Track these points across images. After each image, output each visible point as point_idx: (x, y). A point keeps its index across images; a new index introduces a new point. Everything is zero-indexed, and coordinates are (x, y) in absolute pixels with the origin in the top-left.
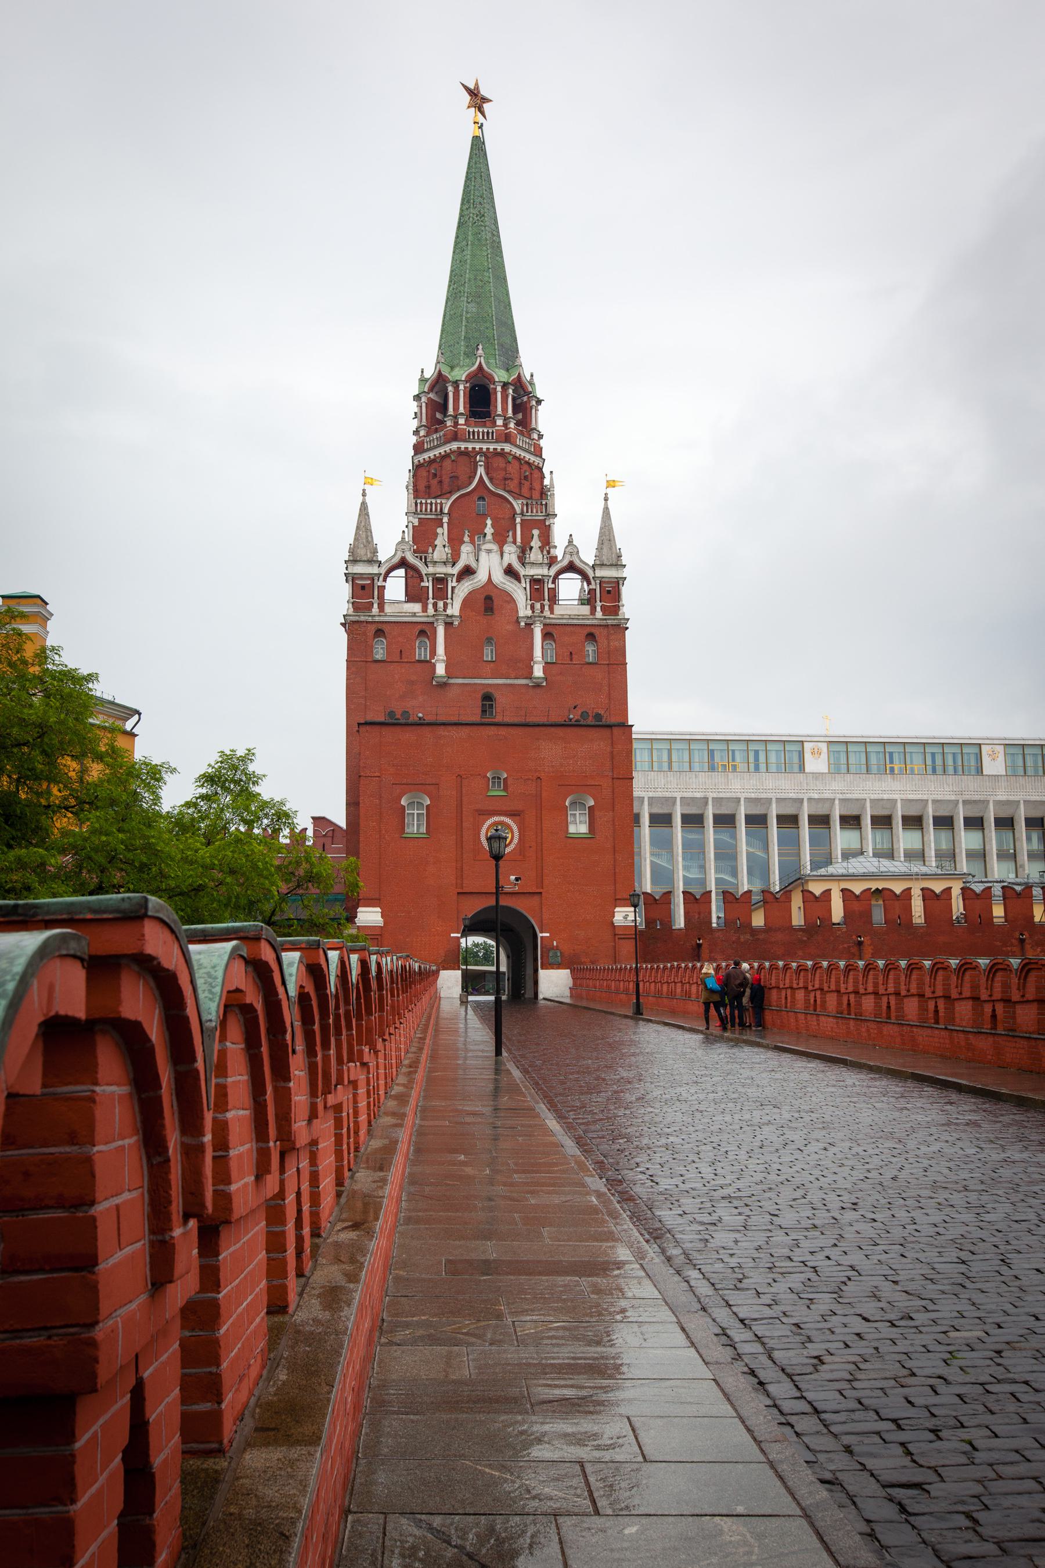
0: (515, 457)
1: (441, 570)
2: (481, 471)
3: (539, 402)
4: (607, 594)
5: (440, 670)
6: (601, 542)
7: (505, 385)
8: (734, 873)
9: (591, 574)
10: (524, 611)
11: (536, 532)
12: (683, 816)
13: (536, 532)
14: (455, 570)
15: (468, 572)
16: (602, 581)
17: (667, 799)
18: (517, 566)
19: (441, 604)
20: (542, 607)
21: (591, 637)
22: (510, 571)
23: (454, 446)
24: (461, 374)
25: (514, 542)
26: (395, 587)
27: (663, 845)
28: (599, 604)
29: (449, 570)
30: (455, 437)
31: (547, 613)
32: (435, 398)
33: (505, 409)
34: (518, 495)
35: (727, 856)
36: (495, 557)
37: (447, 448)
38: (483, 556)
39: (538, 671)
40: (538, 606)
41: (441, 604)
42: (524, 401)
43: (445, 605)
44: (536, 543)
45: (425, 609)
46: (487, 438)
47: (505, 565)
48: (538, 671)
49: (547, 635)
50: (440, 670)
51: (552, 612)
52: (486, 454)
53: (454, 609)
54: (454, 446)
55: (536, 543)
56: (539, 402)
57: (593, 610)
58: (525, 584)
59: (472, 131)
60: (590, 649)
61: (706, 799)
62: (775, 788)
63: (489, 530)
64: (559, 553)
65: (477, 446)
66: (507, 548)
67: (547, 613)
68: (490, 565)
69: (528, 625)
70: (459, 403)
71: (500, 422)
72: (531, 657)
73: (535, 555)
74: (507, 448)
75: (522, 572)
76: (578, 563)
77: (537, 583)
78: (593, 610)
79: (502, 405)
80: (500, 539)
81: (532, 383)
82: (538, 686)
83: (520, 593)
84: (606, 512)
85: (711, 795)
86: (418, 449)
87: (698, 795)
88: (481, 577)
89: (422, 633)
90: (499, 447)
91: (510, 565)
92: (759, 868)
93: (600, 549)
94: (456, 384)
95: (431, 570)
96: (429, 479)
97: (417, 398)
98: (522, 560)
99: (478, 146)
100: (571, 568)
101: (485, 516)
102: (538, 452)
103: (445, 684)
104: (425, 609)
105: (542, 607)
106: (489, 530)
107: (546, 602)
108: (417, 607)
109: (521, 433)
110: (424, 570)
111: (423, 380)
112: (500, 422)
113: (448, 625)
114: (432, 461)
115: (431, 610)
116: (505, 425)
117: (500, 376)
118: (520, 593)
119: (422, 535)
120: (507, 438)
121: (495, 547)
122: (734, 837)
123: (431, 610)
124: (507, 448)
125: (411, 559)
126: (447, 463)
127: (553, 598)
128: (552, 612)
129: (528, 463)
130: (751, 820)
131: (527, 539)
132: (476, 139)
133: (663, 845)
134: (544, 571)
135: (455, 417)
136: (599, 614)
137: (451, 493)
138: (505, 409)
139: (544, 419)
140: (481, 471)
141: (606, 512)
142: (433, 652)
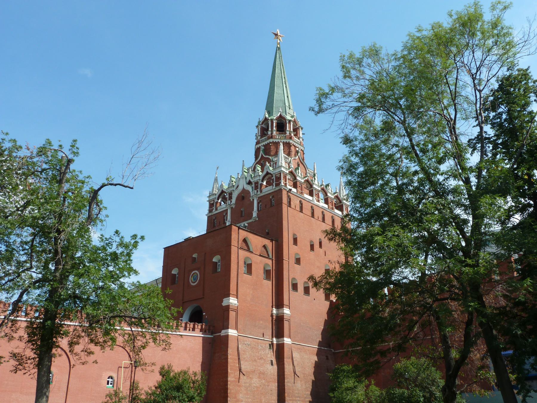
2: (261, 152)
19: (229, 201)
20: (257, 191)
28: (274, 184)
29: (233, 189)
31: (259, 193)
40: (256, 191)
43: (231, 202)
46: (266, 140)
47: (248, 181)
58: (253, 185)
65: (262, 144)
67: (259, 193)
69: (253, 200)
76: (269, 172)
77: (256, 183)
88: (240, 188)
90: (268, 141)
91: (250, 180)
105: (257, 191)
107: (259, 190)
112: (269, 133)
124: (271, 140)
136: (274, 187)
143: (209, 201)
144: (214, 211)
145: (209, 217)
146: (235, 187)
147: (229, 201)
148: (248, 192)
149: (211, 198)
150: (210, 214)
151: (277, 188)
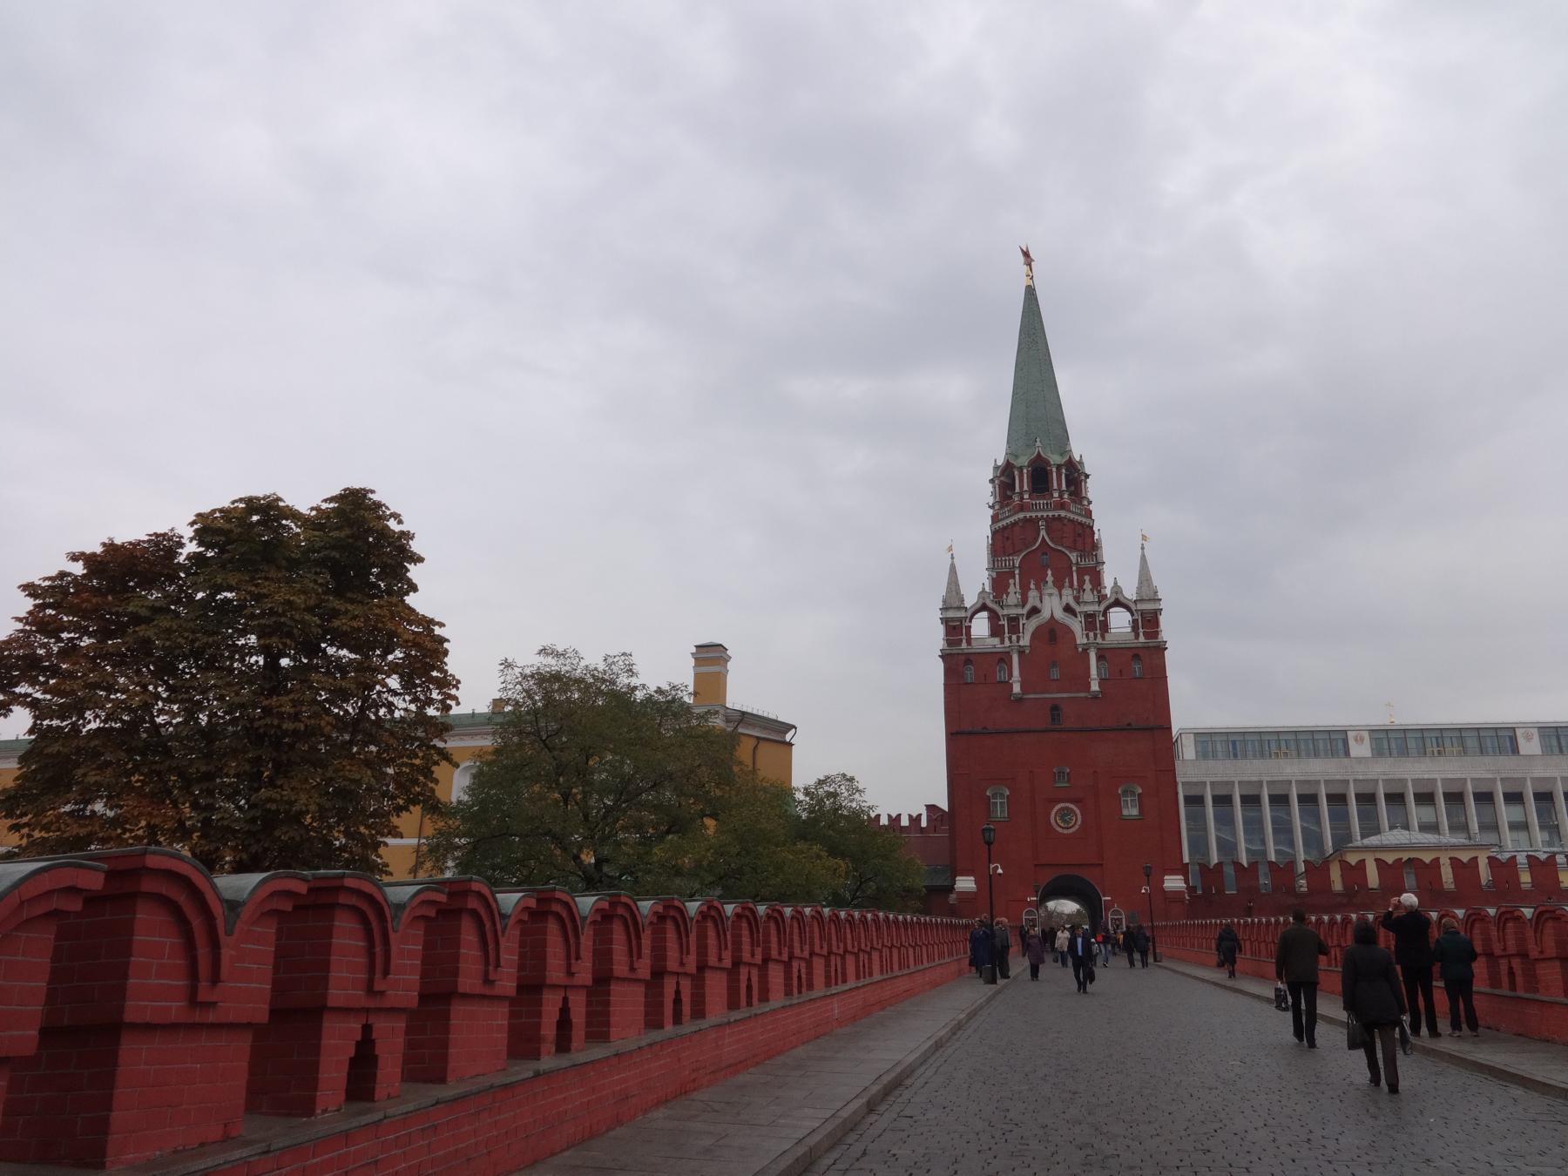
0: (1070, 520)
1: (1013, 612)
2: (1043, 533)
3: (1087, 476)
4: (1148, 621)
5: (1017, 688)
6: (1141, 582)
7: (1059, 467)
8: (1292, 844)
9: (1133, 607)
10: (1081, 639)
11: (1087, 578)
12: (1242, 797)
13: (1087, 578)
14: (1025, 611)
15: (1035, 611)
16: (1143, 613)
17: (1227, 783)
18: (1073, 604)
21: (1136, 657)
22: (1068, 609)
23: (1021, 515)
24: (1023, 461)
25: (1071, 586)
26: (980, 627)
27: (1225, 820)
30: (1022, 508)
32: (1005, 479)
33: (1060, 484)
34: (1073, 548)
35: (1283, 829)
36: (1056, 599)
37: (1016, 517)
38: (1046, 598)
39: (1095, 687)
41: (1014, 637)
42: (1075, 475)
44: (1088, 586)
45: (1002, 642)
46: (1047, 507)
48: (1095, 687)
49: (1100, 658)
50: (1017, 688)
51: (1103, 638)
52: (1047, 519)
53: (1025, 641)
54: (1021, 515)
55: (1088, 586)
56: (1087, 476)
57: (1137, 636)
58: (1081, 618)
59: (1025, 282)
60: (1137, 668)
61: (1261, 783)
62: (1321, 770)
63: (1050, 578)
64: (1108, 592)
66: (1064, 592)
67: (1099, 640)
68: (1052, 605)
69: (1085, 651)
70: (1023, 484)
71: (1056, 495)
72: (1088, 675)
73: (1088, 596)
74: (1063, 513)
75: (1078, 609)
78: (1137, 636)
79: (1058, 482)
80: (1059, 585)
81: (1081, 463)
82: (1095, 698)
83: (1077, 626)
84: (1143, 557)
85: (1265, 779)
86: (995, 519)
87: (1254, 779)
88: (1046, 614)
89: (1001, 660)
92: (1313, 839)
93: (1139, 588)
94: (1021, 469)
95: (1005, 612)
96: (1003, 542)
97: (992, 481)
98: (1077, 599)
99: (1030, 292)
100: (1117, 603)
101: (1044, 568)
102: (1089, 514)
103: (1019, 700)
104: (1002, 642)
106: (1050, 578)
108: (996, 641)
109: (1074, 501)
110: (1001, 612)
111: (996, 468)
112: (1056, 495)
113: (1021, 653)
114: (1005, 528)
115: (1007, 643)
116: (1061, 496)
117: (1055, 459)
118: (1077, 626)
119: (999, 584)
120: (1062, 506)
121: (1055, 591)
122: (1289, 814)
123: (1007, 643)
124: (1063, 513)
125: (991, 605)
126: (1017, 529)
127: (1105, 627)
128: (1103, 638)
129: (1080, 524)
130: (1302, 799)
131: (1081, 583)
132: (1028, 287)
133: (1225, 820)
134: (1096, 608)
135: (1021, 494)
136: (1142, 639)
137: (1020, 551)
138: (1060, 484)
139: (1093, 489)
140: (1043, 533)
141: (1143, 557)
142: (1011, 675)
143: (945, 621)
144: (964, 645)
145: (944, 656)
146: (1028, 607)
147: (1014, 637)
148: (1068, 631)
149: (951, 614)
150: (955, 650)
151: (1152, 642)
